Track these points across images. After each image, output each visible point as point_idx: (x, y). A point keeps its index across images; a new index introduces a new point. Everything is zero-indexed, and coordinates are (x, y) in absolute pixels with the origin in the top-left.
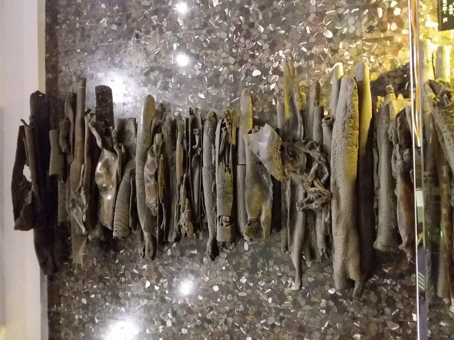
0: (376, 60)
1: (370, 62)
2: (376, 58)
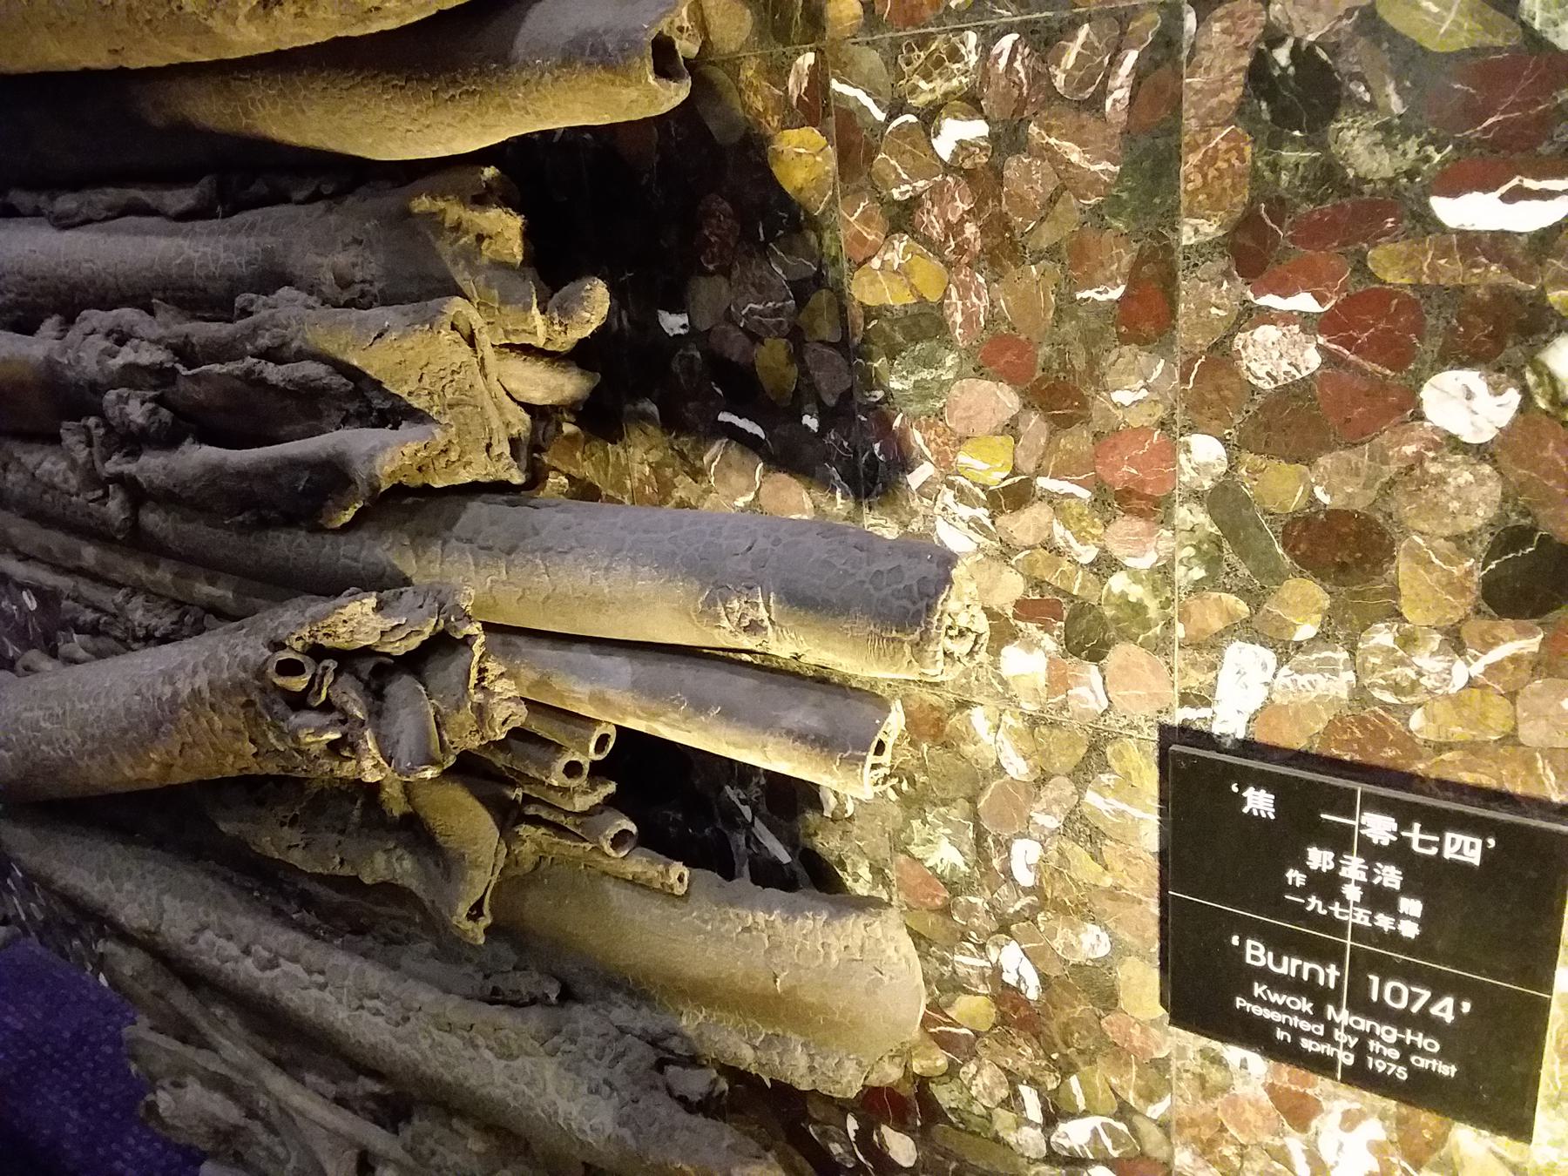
0: (948, 168)
1: (930, 117)
2: (970, 175)
